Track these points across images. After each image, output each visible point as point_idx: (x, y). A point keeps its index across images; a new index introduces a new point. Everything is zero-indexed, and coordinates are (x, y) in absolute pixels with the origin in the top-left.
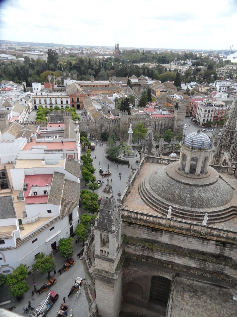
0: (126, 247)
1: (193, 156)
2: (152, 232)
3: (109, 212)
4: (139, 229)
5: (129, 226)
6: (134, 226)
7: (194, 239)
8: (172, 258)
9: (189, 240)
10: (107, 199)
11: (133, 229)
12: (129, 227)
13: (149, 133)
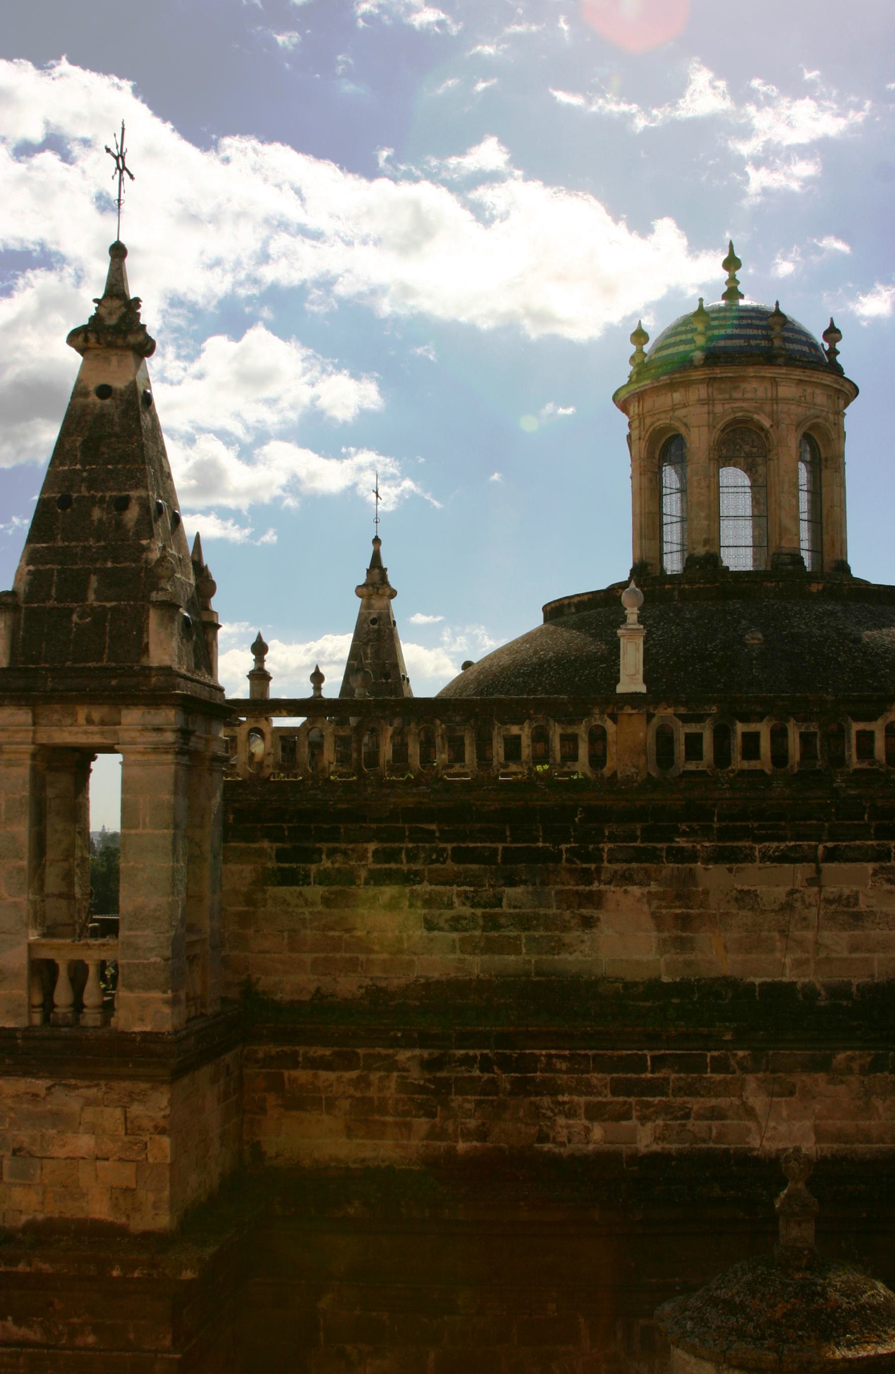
0: (272, 1100)
1: (724, 410)
2: (509, 891)
3: (123, 504)
4: (389, 891)
5: (288, 878)
6: (339, 863)
7: (870, 867)
8: (716, 1114)
9: (831, 890)
10: (108, 402)
11: (327, 901)
12: (284, 891)
13: (374, 621)
